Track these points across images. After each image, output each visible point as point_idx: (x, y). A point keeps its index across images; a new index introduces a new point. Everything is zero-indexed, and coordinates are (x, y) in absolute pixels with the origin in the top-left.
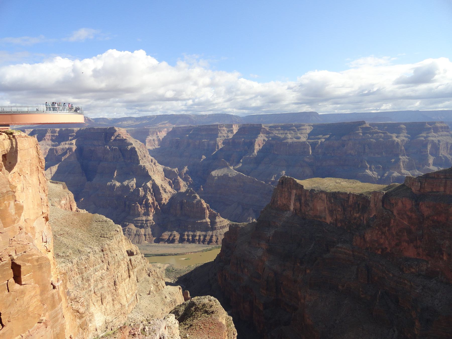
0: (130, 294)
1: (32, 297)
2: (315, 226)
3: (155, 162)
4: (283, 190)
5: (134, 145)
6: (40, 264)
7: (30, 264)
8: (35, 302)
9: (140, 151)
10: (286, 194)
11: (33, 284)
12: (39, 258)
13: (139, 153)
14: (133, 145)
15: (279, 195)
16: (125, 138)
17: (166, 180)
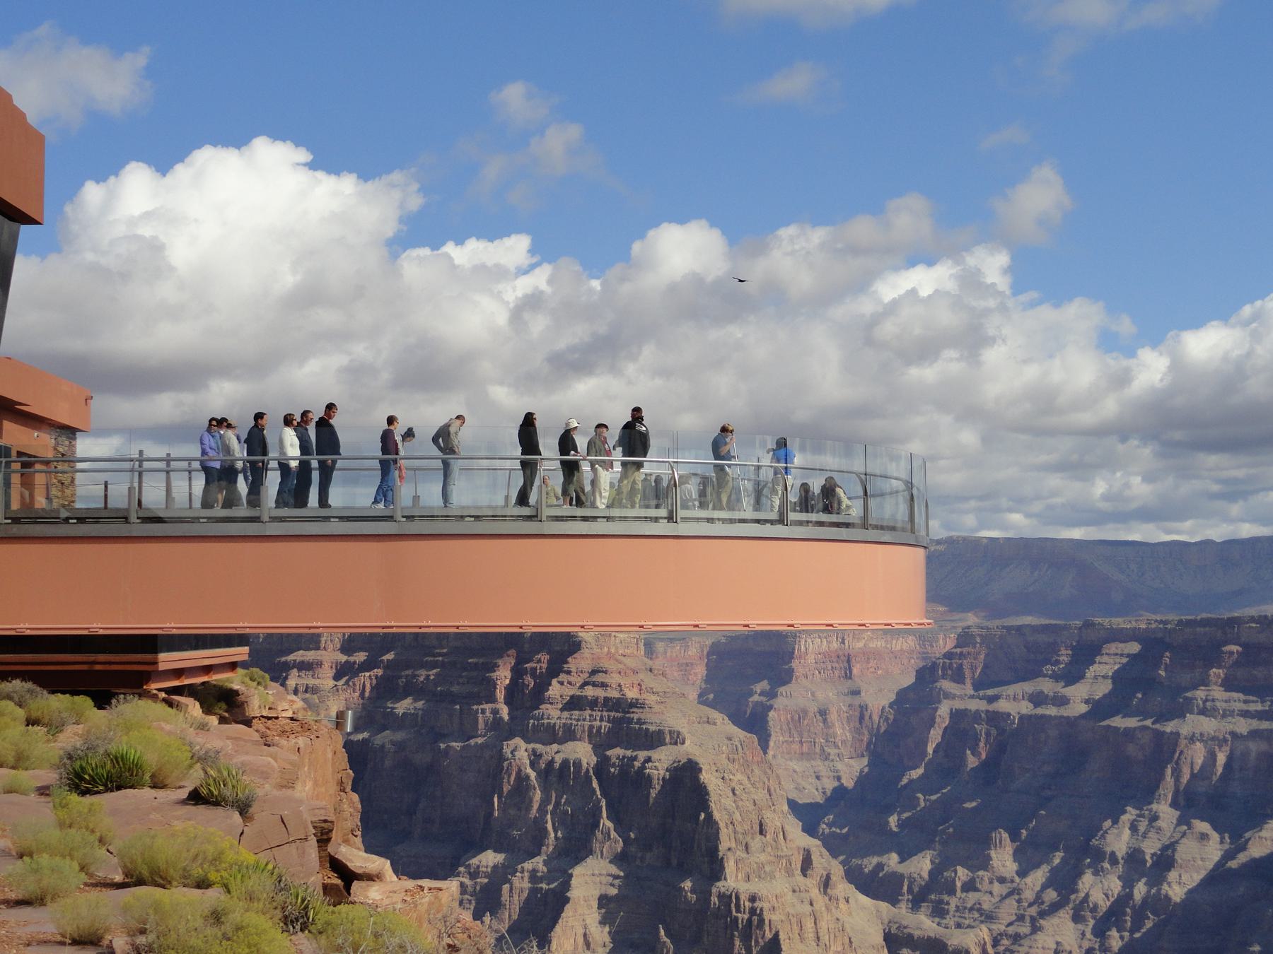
3: (828, 877)
5: (690, 749)
9: (733, 790)
13: (721, 805)
14: (683, 743)
16: (631, 694)
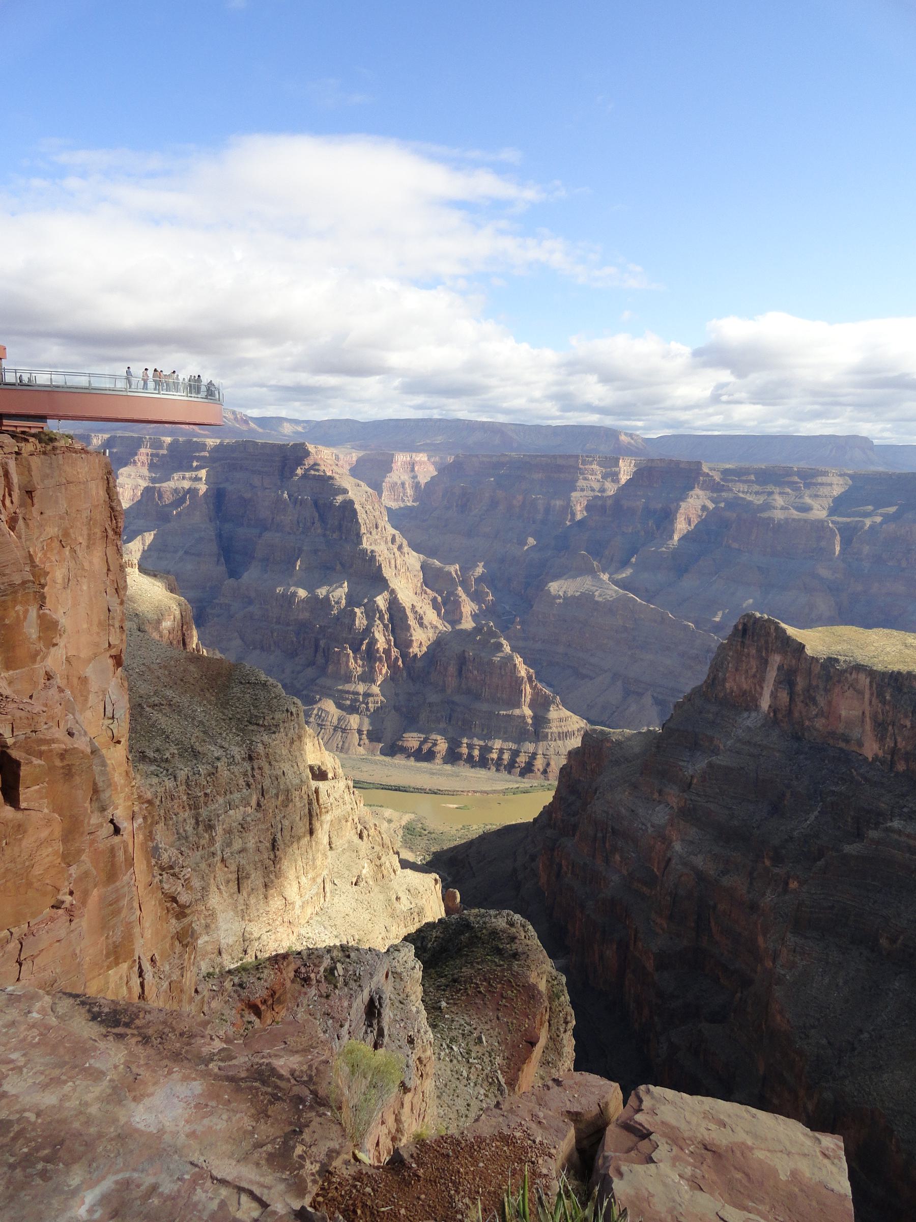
0: (310, 876)
1: (41, 844)
2: (826, 762)
3: (402, 544)
4: (746, 650)
5: (351, 495)
6: (68, 765)
7: (43, 763)
8: (49, 855)
9: (366, 512)
10: (754, 663)
11: (46, 811)
12: (66, 750)
13: (362, 517)
15: (730, 665)
17: (426, 593)
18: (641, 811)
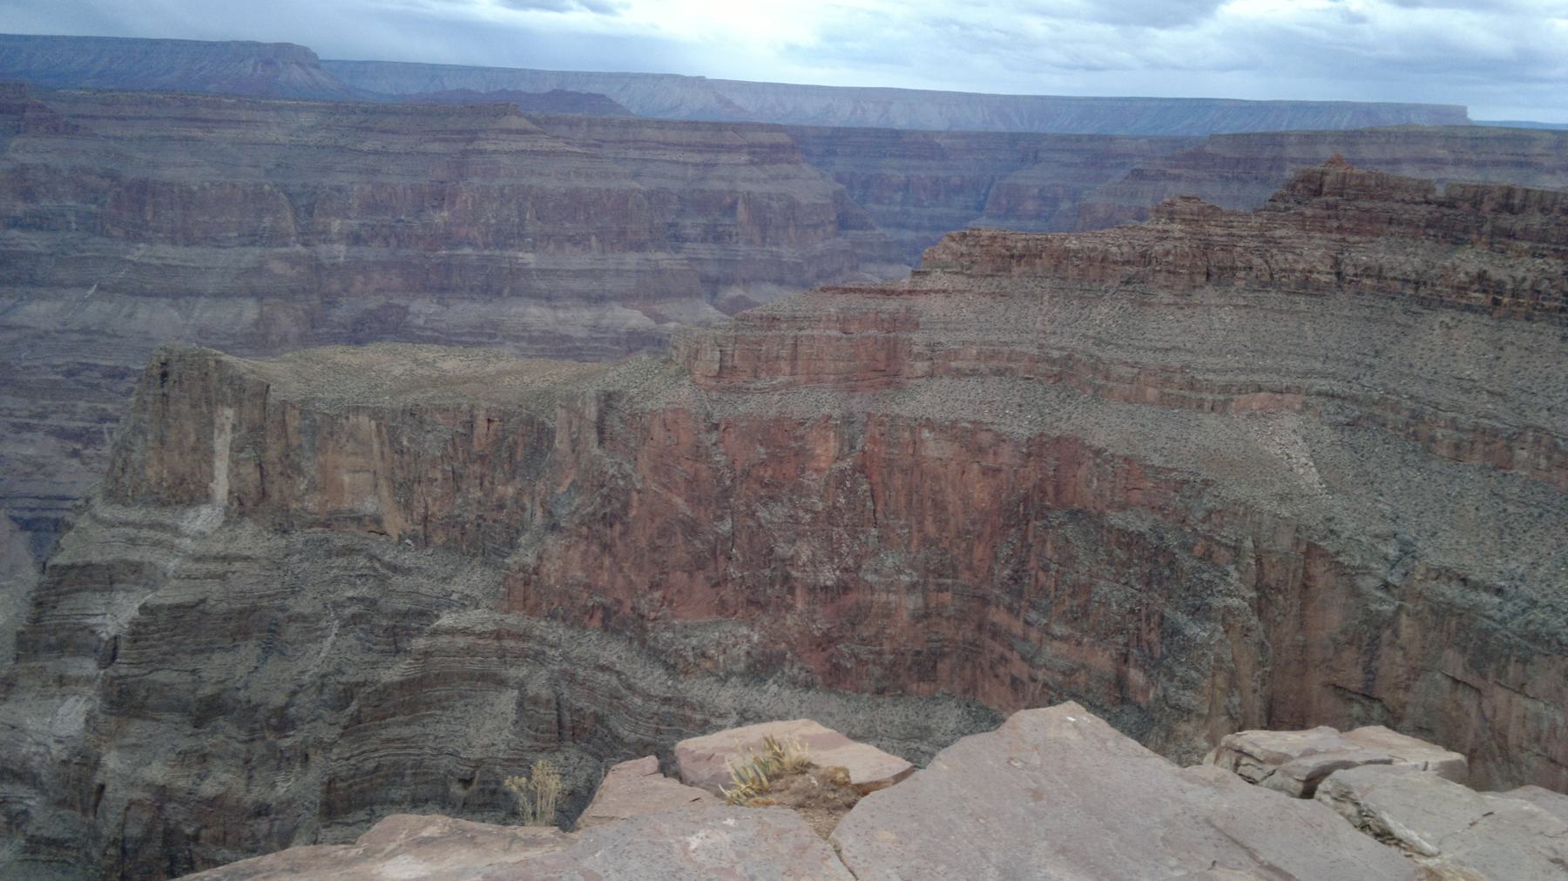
4: (172, 408)
10: (190, 426)
18: (31, 723)
